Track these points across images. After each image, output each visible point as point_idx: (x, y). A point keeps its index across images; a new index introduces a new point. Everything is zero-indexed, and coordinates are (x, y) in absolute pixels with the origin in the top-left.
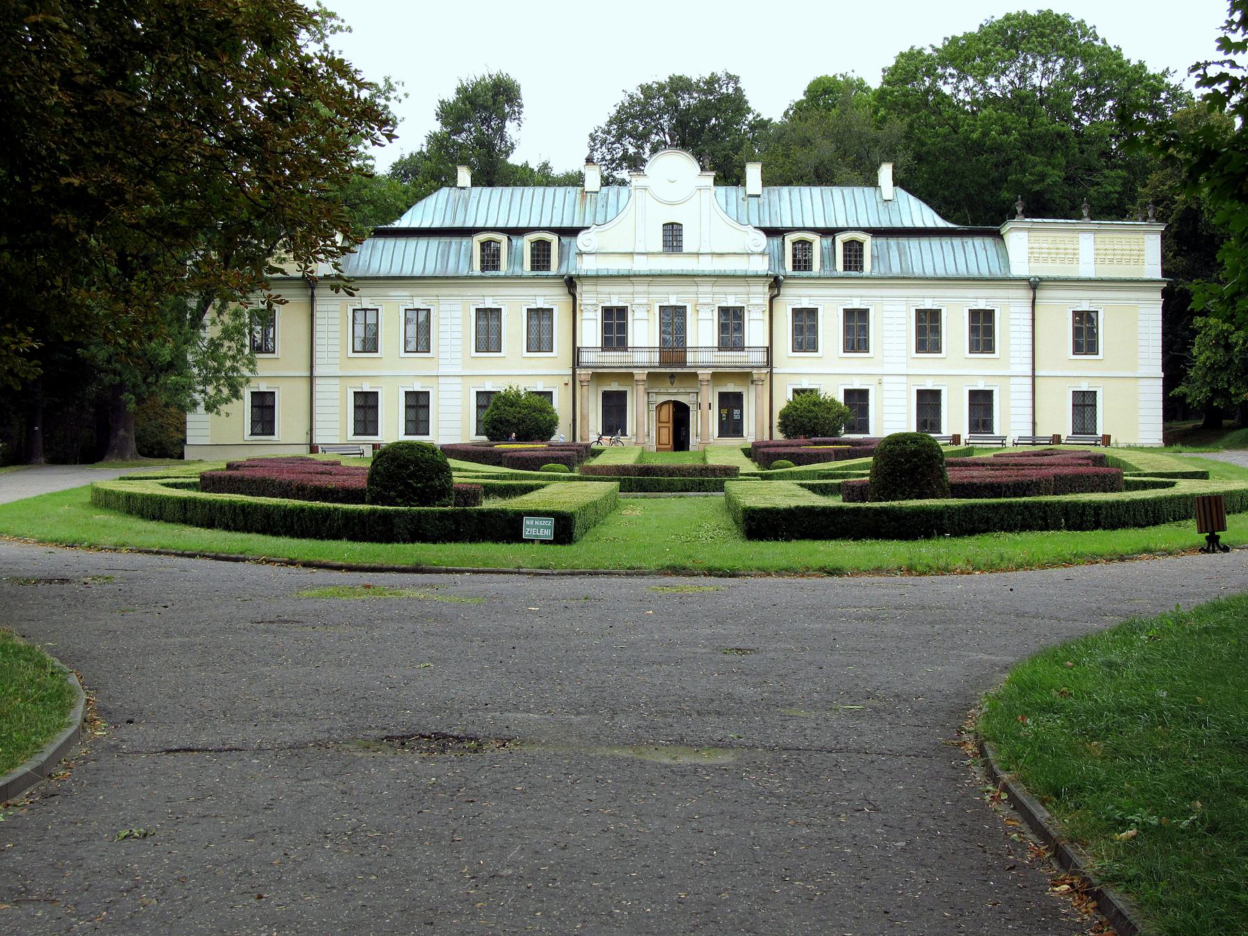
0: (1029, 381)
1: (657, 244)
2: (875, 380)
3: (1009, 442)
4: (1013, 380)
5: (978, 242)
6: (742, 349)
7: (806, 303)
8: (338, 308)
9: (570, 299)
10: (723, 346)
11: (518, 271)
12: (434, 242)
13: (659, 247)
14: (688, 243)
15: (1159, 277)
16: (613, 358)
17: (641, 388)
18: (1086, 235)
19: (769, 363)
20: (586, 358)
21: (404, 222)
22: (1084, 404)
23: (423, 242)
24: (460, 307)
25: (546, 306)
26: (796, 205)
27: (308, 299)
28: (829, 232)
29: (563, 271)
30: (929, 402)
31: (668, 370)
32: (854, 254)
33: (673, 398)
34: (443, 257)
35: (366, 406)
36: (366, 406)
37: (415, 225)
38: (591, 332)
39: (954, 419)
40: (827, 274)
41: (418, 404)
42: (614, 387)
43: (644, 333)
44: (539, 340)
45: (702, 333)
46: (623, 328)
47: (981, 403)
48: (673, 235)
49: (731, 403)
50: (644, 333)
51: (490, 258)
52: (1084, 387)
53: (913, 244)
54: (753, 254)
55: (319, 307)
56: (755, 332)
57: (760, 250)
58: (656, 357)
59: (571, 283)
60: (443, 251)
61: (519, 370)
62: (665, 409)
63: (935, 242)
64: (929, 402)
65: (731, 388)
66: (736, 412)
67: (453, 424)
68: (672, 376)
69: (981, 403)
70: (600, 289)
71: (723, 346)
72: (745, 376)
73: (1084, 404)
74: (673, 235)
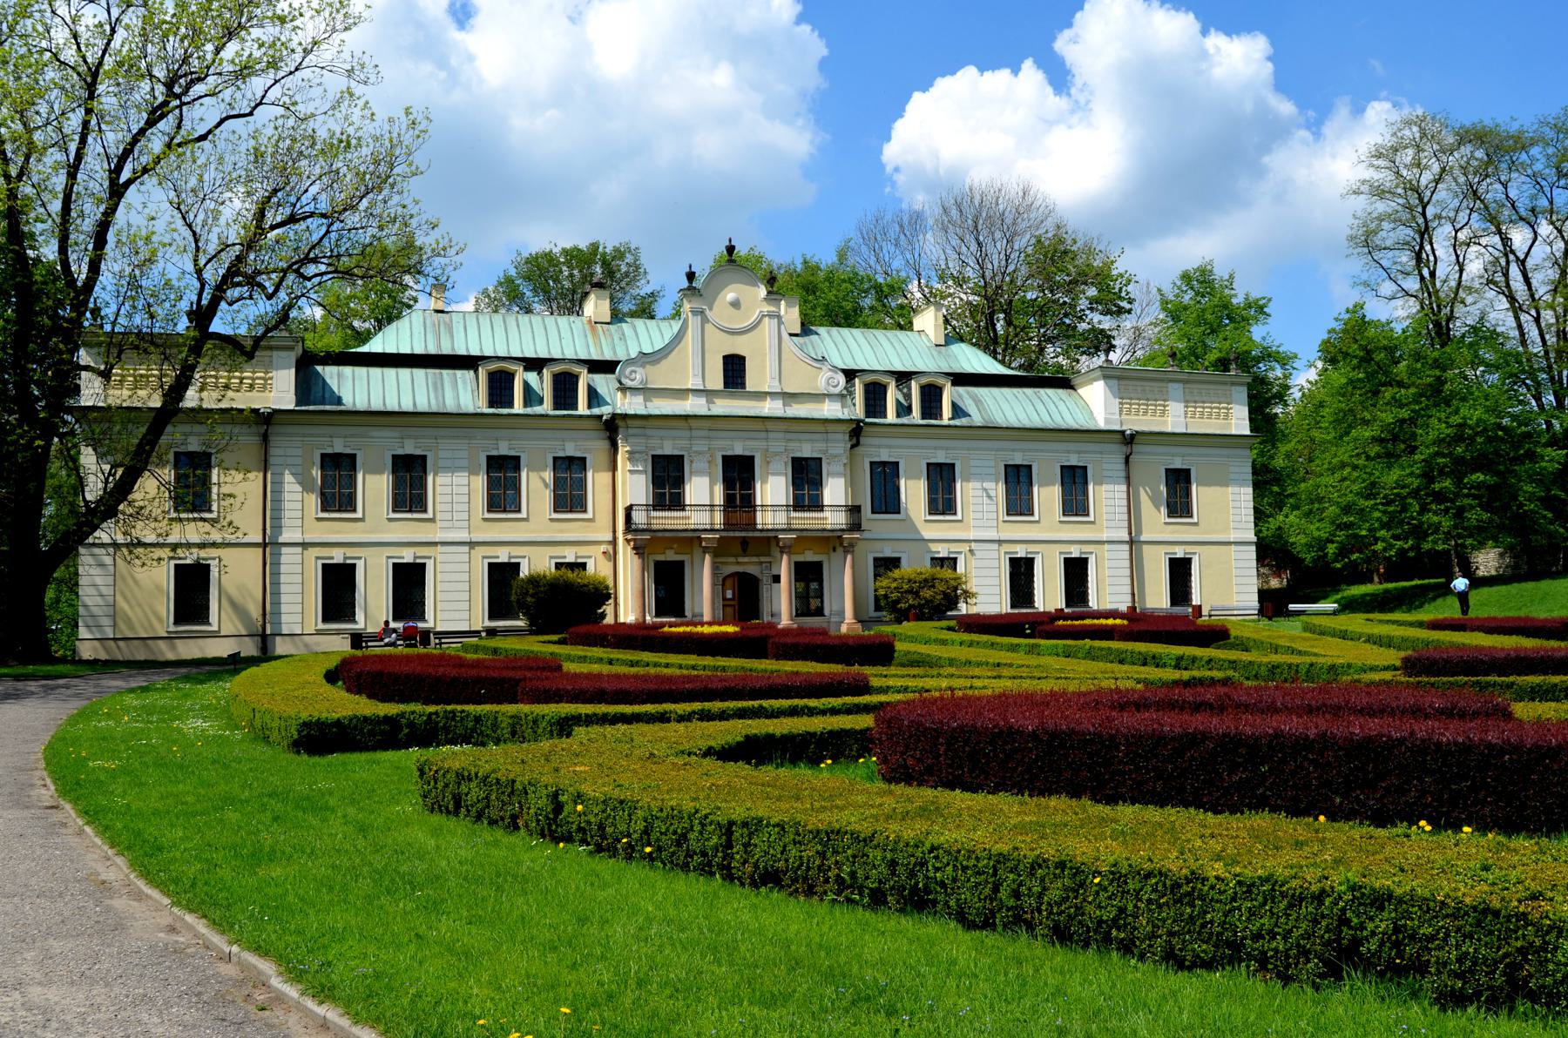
0: (1127, 547)
1: (716, 380)
2: (965, 548)
3: (1205, 612)
4: (1106, 546)
5: (1050, 391)
6: (819, 507)
7: (885, 456)
8: (299, 452)
9: (605, 444)
10: (798, 505)
11: (538, 410)
12: (420, 373)
13: (720, 385)
14: (752, 383)
15: (1248, 432)
16: (667, 520)
17: (708, 558)
18: (1176, 385)
19: (855, 526)
20: (639, 518)
21: (375, 346)
22: (1180, 571)
23: (405, 373)
24: (465, 454)
25: (578, 454)
26: (843, 348)
27: (256, 439)
28: (903, 377)
29: (596, 411)
30: (1021, 572)
31: (737, 534)
32: (931, 396)
33: (740, 569)
34: (436, 389)
35: (338, 588)
36: (338, 588)
37: (391, 349)
38: (634, 486)
39: (1049, 595)
40: (905, 420)
41: (409, 583)
42: (671, 556)
43: (703, 491)
44: (569, 498)
45: (772, 491)
46: (679, 482)
47: (1076, 571)
48: (734, 369)
49: (809, 576)
50: (703, 491)
51: (500, 387)
52: (1180, 552)
53: (983, 392)
54: (829, 396)
55: (272, 451)
56: (834, 491)
57: (837, 390)
58: (719, 518)
59: (612, 427)
60: (435, 384)
61: (539, 539)
62: (729, 582)
63: (1007, 391)
64: (1021, 572)
65: (809, 556)
66: (814, 586)
67: (457, 604)
68: (745, 543)
69: (1076, 571)
70: (649, 432)
71: (798, 505)
72: (832, 541)
73: (1180, 571)
74: (734, 369)
